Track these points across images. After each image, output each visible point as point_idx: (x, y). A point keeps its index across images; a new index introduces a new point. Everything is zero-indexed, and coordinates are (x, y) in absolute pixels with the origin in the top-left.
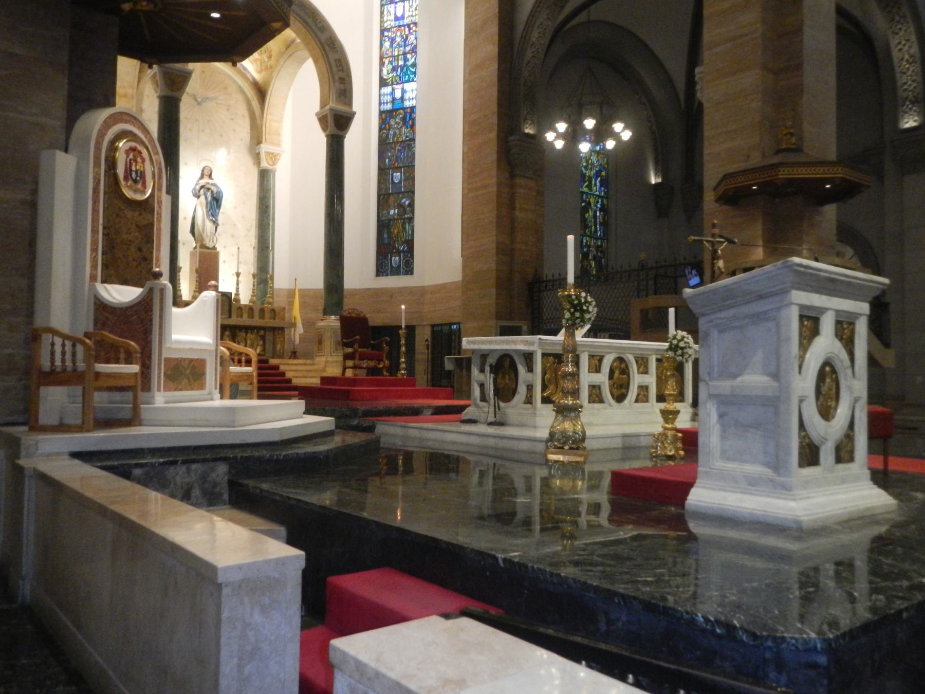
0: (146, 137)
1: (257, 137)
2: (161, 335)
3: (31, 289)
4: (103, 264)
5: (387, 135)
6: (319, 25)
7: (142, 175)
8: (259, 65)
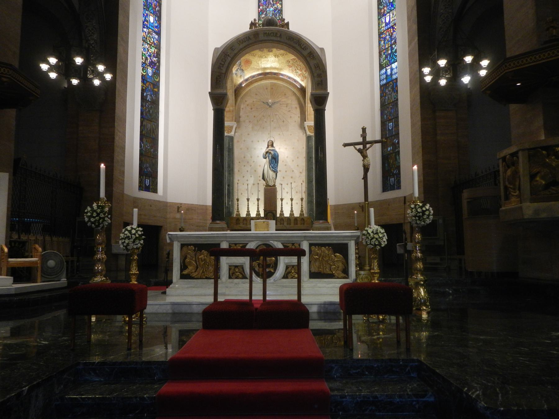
5: (385, 100)
6: (302, 47)
8: (302, 77)
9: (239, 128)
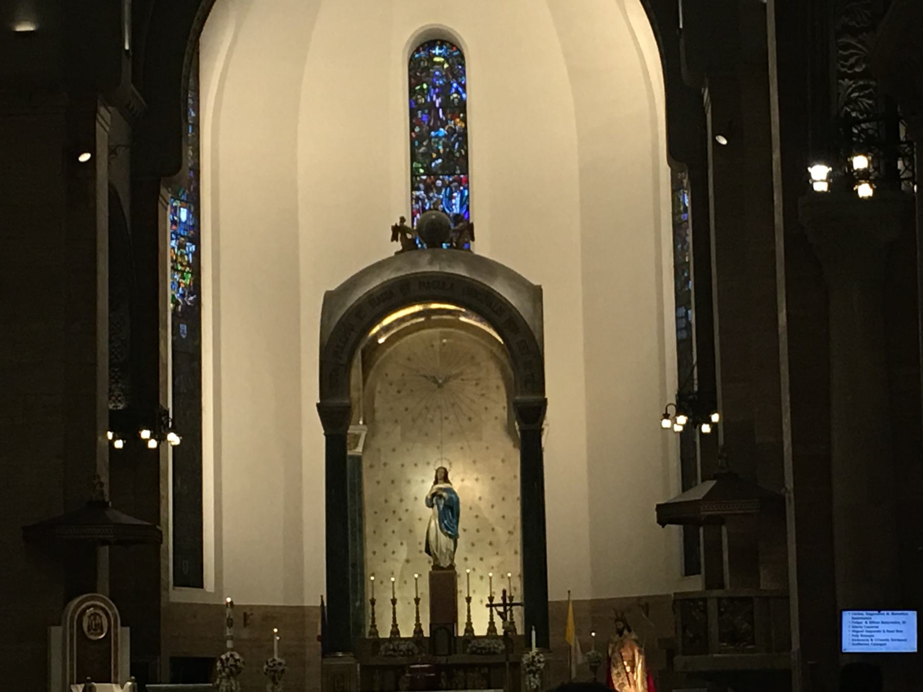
6: (495, 309)
9: (373, 435)
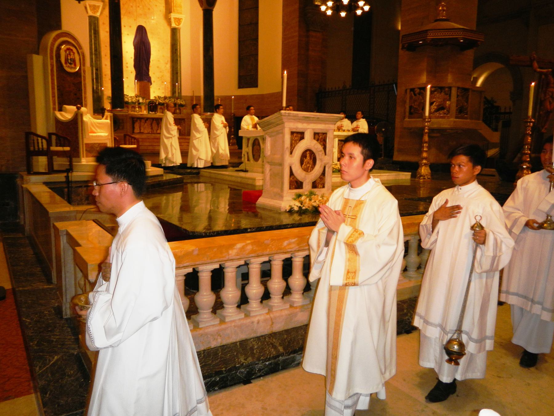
0: (75, 42)
1: (169, 10)
2: (82, 134)
3: (29, 115)
4: (58, 103)
7: (74, 61)
